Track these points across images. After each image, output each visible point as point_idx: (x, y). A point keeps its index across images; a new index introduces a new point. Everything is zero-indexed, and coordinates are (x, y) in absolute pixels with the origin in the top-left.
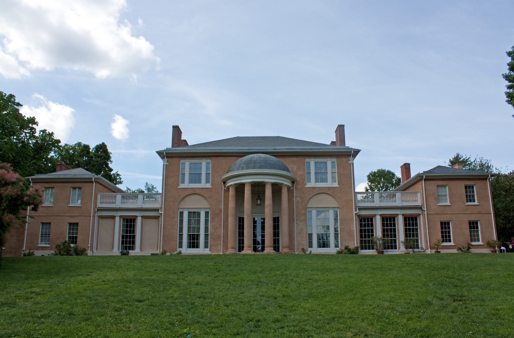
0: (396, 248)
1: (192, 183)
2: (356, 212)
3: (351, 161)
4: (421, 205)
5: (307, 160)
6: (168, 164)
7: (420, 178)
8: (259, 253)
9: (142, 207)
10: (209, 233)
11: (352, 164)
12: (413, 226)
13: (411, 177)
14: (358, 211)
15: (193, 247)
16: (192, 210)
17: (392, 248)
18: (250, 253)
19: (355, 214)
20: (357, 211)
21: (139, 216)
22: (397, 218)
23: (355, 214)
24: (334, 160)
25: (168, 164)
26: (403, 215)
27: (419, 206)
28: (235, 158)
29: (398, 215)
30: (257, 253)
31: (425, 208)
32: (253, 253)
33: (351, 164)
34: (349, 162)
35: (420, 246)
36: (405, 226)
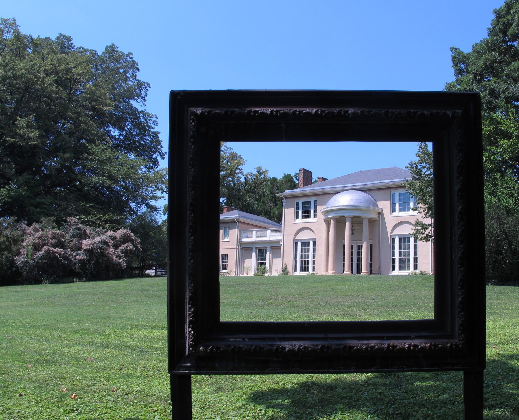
15: (305, 271)
16: (304, 241)
25: (286, 204)
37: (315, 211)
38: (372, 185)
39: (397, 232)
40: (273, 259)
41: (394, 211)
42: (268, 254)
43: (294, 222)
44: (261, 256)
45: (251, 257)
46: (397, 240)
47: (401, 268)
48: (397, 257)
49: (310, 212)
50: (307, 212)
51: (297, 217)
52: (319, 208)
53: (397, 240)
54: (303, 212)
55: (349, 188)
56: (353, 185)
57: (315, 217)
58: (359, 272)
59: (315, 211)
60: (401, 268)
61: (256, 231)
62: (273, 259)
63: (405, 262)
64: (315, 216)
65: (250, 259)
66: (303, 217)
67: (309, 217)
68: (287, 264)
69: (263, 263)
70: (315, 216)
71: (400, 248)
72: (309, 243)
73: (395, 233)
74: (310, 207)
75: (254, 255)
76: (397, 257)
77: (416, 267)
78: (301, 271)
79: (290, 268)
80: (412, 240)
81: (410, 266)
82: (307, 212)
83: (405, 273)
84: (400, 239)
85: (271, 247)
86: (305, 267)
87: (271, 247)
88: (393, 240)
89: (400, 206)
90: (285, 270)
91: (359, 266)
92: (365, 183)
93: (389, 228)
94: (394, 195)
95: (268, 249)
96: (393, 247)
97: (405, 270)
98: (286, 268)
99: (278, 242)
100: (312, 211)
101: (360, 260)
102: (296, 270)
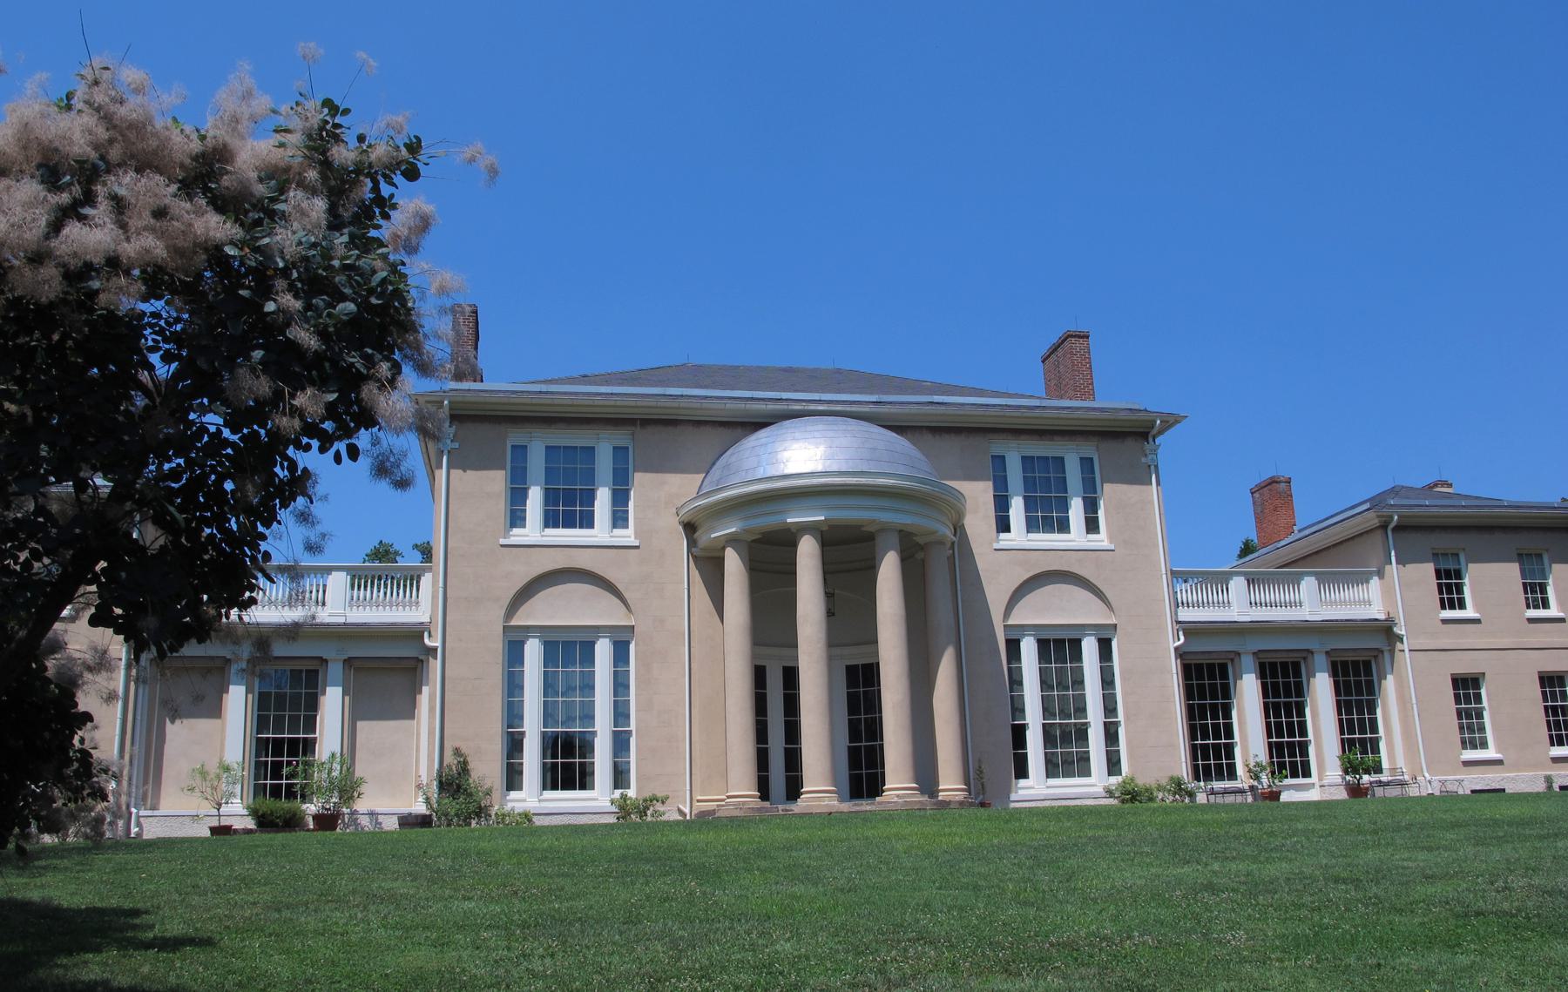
0: (1307, 774)
1: (556, 526)
2: (1177, 644)
3: (1150, 457)
4: (1382, 616)
5: (998, 446)
6: (456, 445)
7: (1372, 520)
8: (868, 808)
9: (348, 621)
10: (633, 727)
11: (1152, 467)
12: (1360, 693)
13: (1301, 522)
14: (1182, 639)
15: (568, 785)
17: (1294, 775)
18: (834, 805)
19: (1176, 649)
20: (1179, 640)
21: (335, 660)
22: (1306, 667)
23: (1176, 649)
24: (1089, 449)
25: (456, 445)
26: (1327, 653)
27: (1376, 620)
28: (739, 431)
29: (1310, 652)
30: (863, 808)
31: (1403, 628)
32: (846, 807)
33: (1149, 466)
34: (1143, 460)
35: (1385, 765)
36: (1336, 695)
37: (1091, 506)
38: (907, 409)
39: (1032, 612)
40: (360, 724)
41: (1004, 525)
42: (332, 702)
43: (503, 541)
44: (280, 705)
45: (216, 711)
46: (1029, 648)
47: (1052, 769)
48: (1033, 718)
49: (589, 497)
50: (570, 498)
51: (517, 518)
52: (642, 483)
53: (1029, 648)
54: (550, 497)
55: (812, 407)
56: (816, 396)
57: (615, 526)
58: (794, 789)
59: (1091, 506)
60: (1052, 769)
61: (1316, 574)
62: (360, 724)
63: (1066, 739)
64: (619, 519)
65: (203, 725)
66: (551, 520)
67: (587, 521)
68: (464, 750)
69: (293, 743)
70: (1092, 525)
71: (549, 686)
72: (1076, 644)
73: (1019, 617)
74: (590, 476)
75: (237, 699)
76: (1033, 718)
77: (1113, 765)
78: (544, 788)
79: (487, 769)
80: (1089, 647)
81: (1088, 759)
82: (570, 498)
83: (1069, 788)
84: (1043, 645)
85: (349, 662)
86: (568, 768)
87: (349, 662)
88: (1013, 646)
89: (1029, 505)
90: (453, 783)
91: (793, 760)
92: (874, 398)
93: (996, 597)
94: (1000, 461)
95: (335, 670)
96: (1016, 681)
97: (1068, 774)
98: (464, 769)
99: (414, 634)
100: (603, 499)
101: (792, 732)
102: (513, 779)
